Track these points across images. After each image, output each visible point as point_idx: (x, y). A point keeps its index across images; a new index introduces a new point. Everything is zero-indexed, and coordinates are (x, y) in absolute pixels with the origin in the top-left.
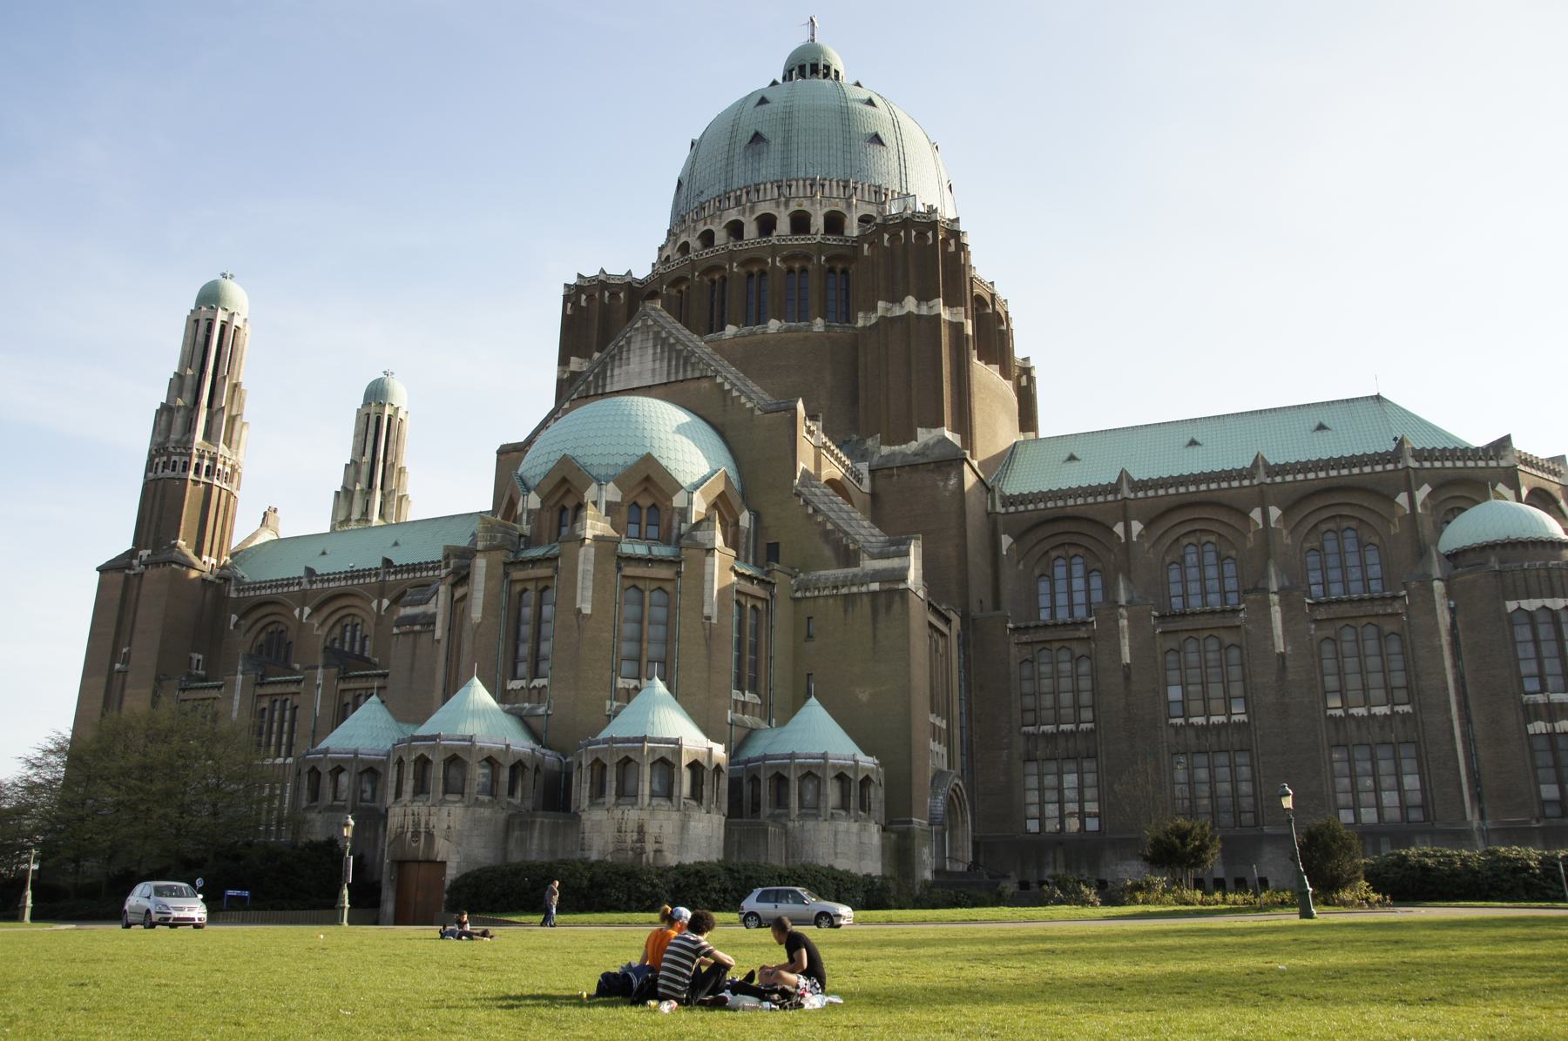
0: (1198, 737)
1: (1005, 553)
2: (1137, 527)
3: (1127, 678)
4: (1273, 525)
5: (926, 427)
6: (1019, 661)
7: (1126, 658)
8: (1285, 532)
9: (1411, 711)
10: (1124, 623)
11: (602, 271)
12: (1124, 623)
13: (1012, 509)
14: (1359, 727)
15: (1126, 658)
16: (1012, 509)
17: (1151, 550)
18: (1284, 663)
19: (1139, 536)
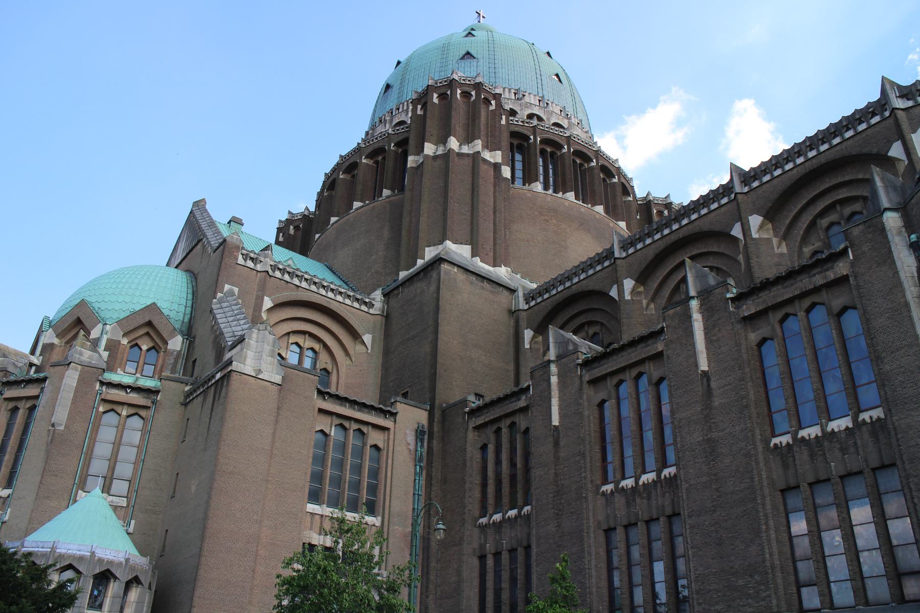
0: (628, 504)
1: (527, 346)
2: (628, 284)
3: (556, 444)
4: (755, 235)
5: (434, 245)
6: (479, 446)
7: (556, 421)
8: (775, 241)
9: (882, 416)
10: (554, 380)
11: (290, 212)
12: (554, 380)
13: (533, 303)
14: (812, 456)
15: (556, 421)
16: (533, 303)
17: (652, 306)
18: (709, 385)
19: (633, 292)
